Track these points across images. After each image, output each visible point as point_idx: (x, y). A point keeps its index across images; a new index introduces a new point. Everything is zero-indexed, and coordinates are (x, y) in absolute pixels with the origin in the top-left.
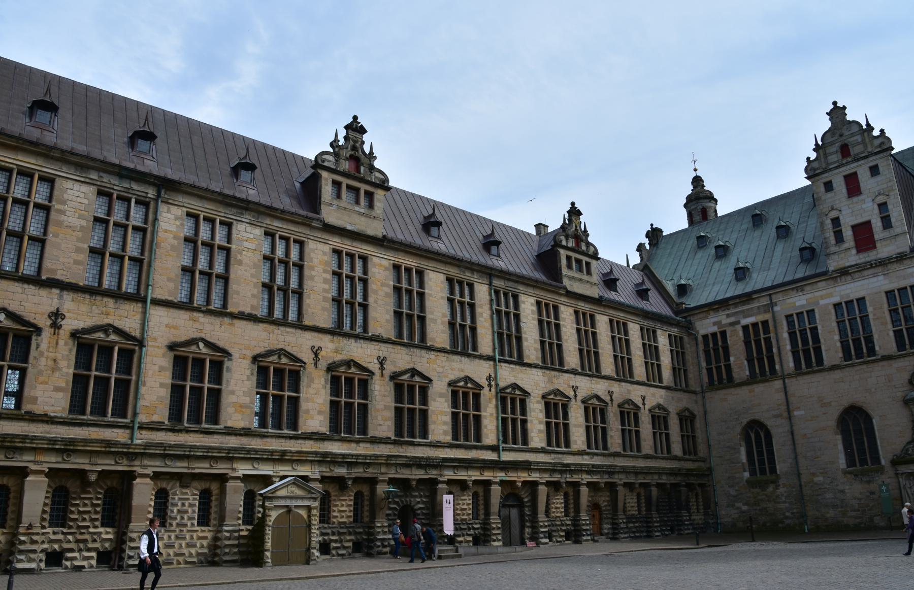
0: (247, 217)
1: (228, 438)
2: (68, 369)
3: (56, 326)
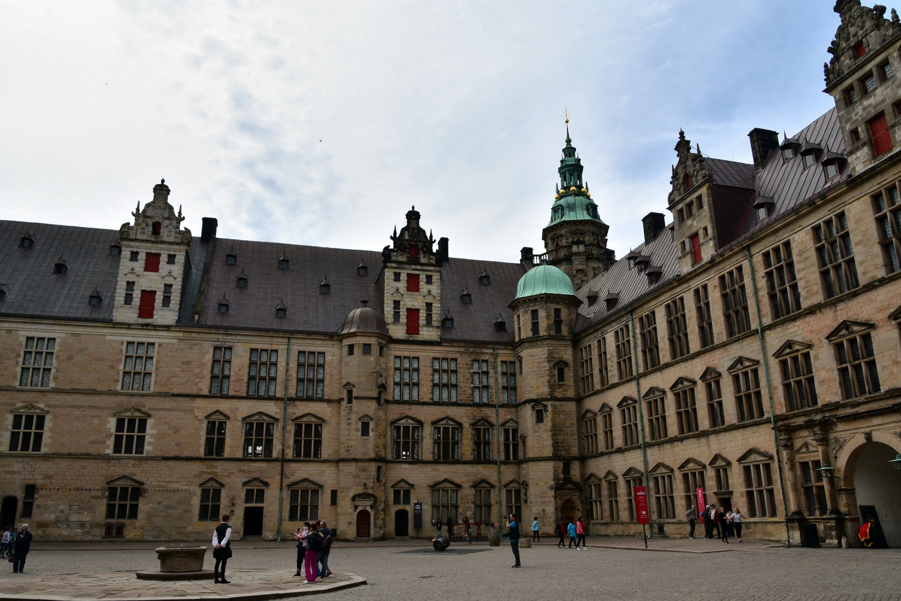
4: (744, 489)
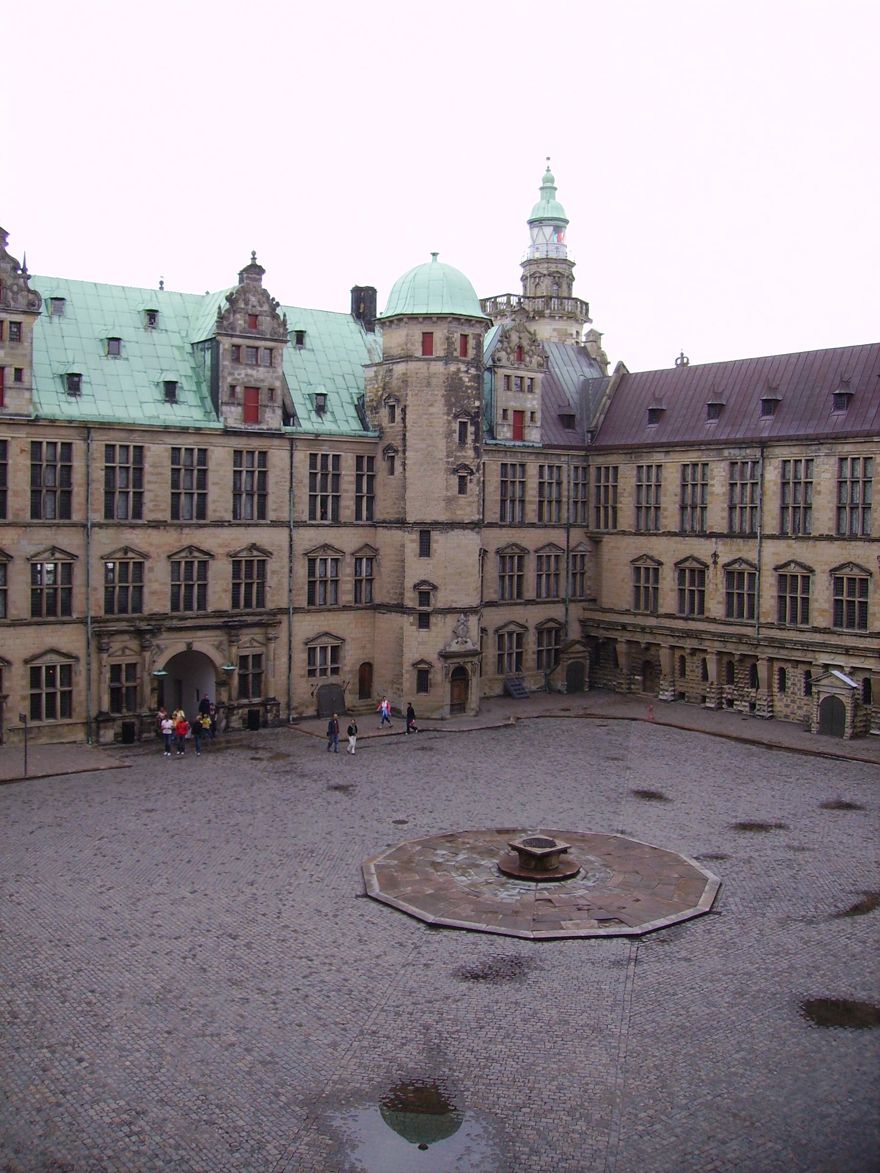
0: (824, 450)
1: (815, 635)
2: (723, 590)
3: (715, 563)
4: (29, 692)
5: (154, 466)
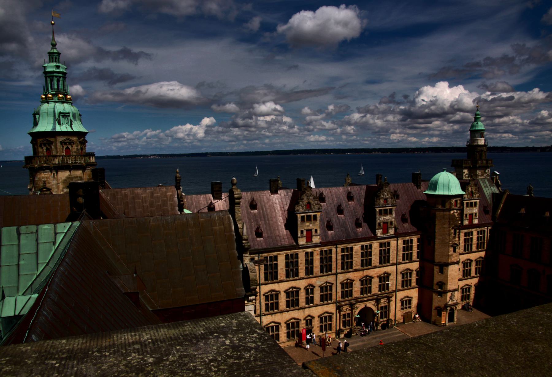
5: (356, 252)
